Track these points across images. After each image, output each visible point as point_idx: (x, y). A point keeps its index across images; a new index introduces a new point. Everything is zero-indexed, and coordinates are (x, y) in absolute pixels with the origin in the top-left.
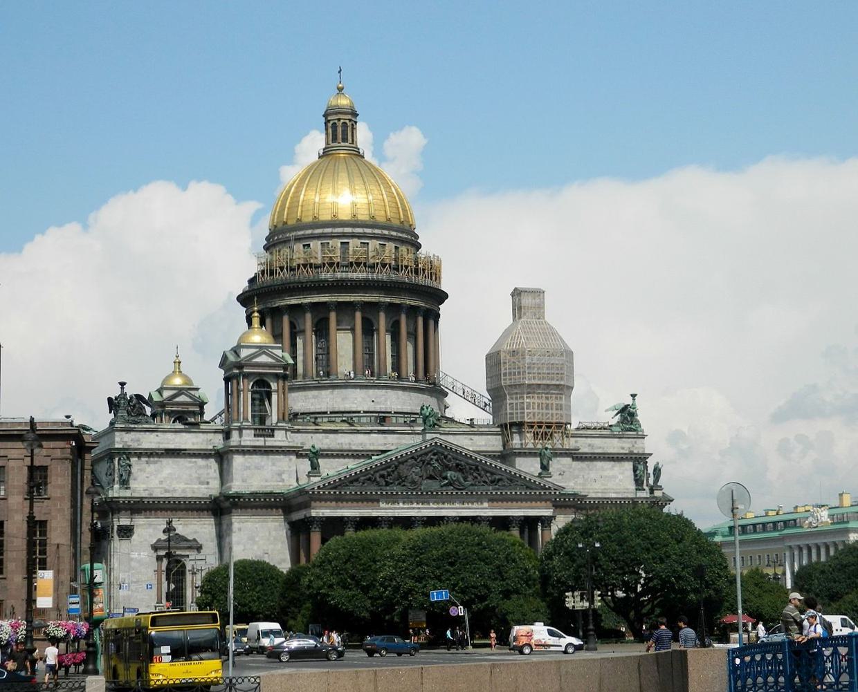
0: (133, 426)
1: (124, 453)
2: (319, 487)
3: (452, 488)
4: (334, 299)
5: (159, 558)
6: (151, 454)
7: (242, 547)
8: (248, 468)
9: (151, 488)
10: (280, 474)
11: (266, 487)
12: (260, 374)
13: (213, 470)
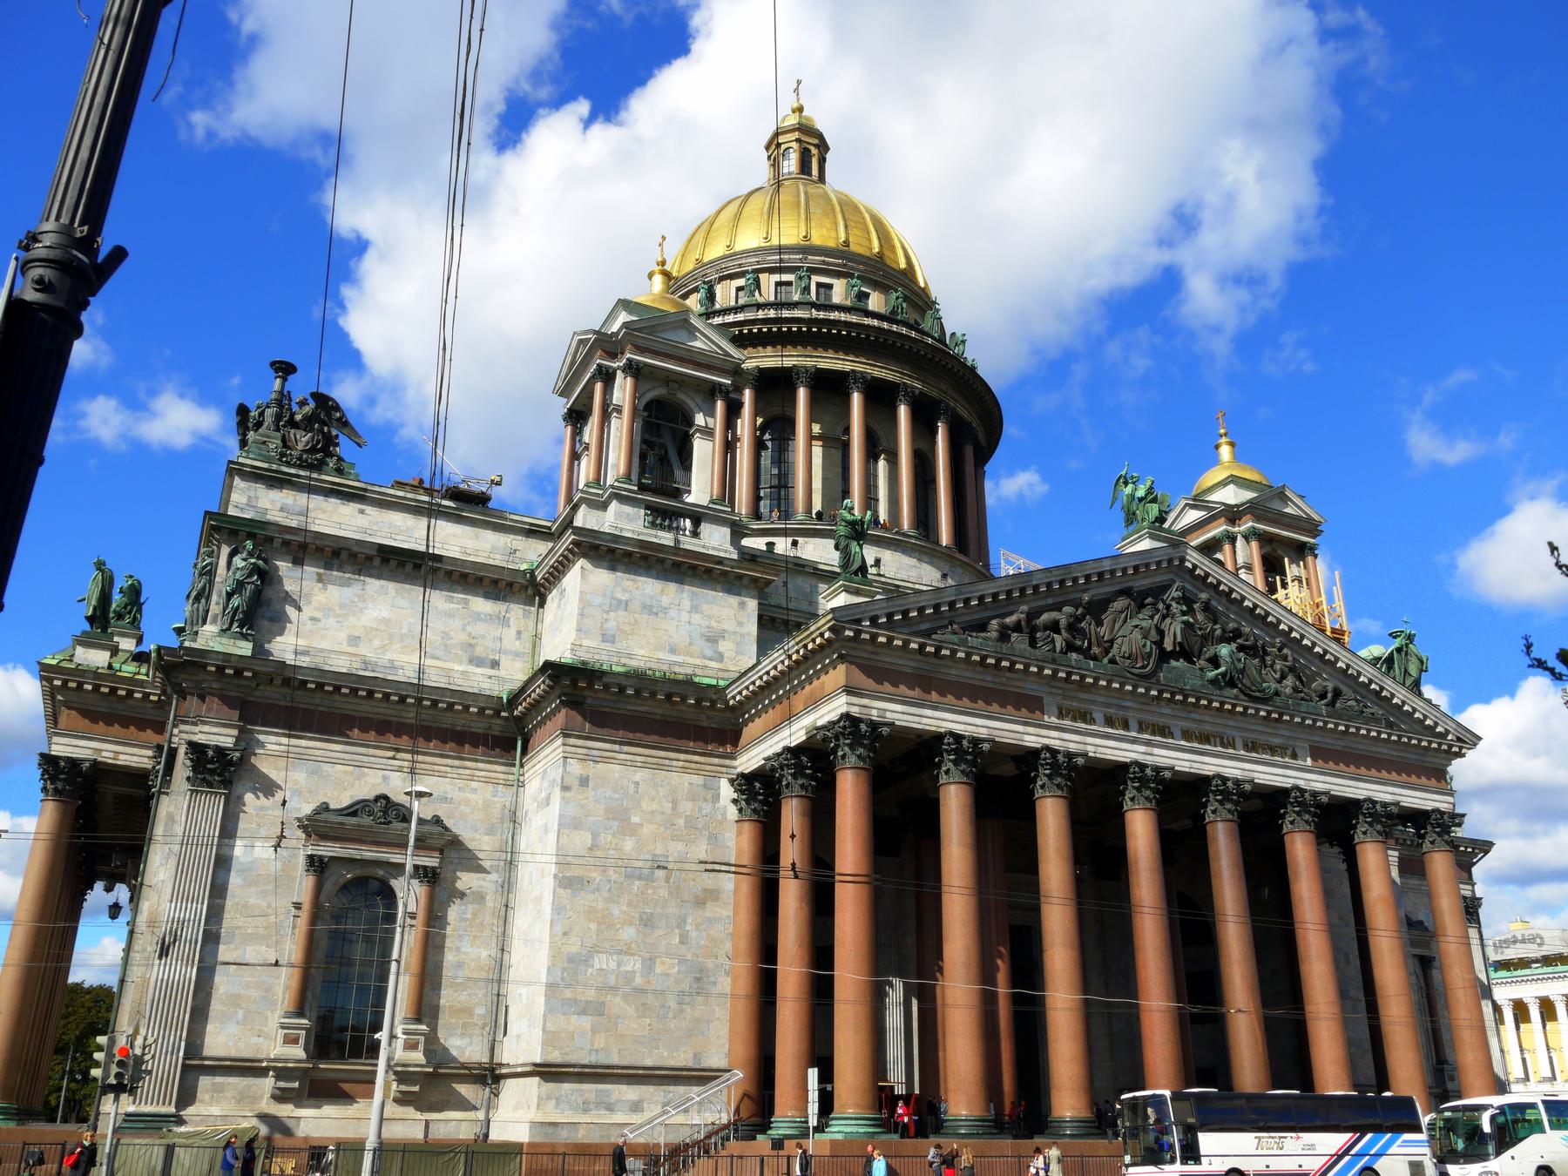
0: (293, 471)
1: (251, 536)
2: (874, 620)
3: (1235, 691)
4: (809, 363)
5: (317, 865)
6: (336, 553)
7: (587, 839)
8: (625, 605)
9: (323, 650)
10: (713, 639)
11: (676, 663)
12: (668, 378)
13: (512, 632)
